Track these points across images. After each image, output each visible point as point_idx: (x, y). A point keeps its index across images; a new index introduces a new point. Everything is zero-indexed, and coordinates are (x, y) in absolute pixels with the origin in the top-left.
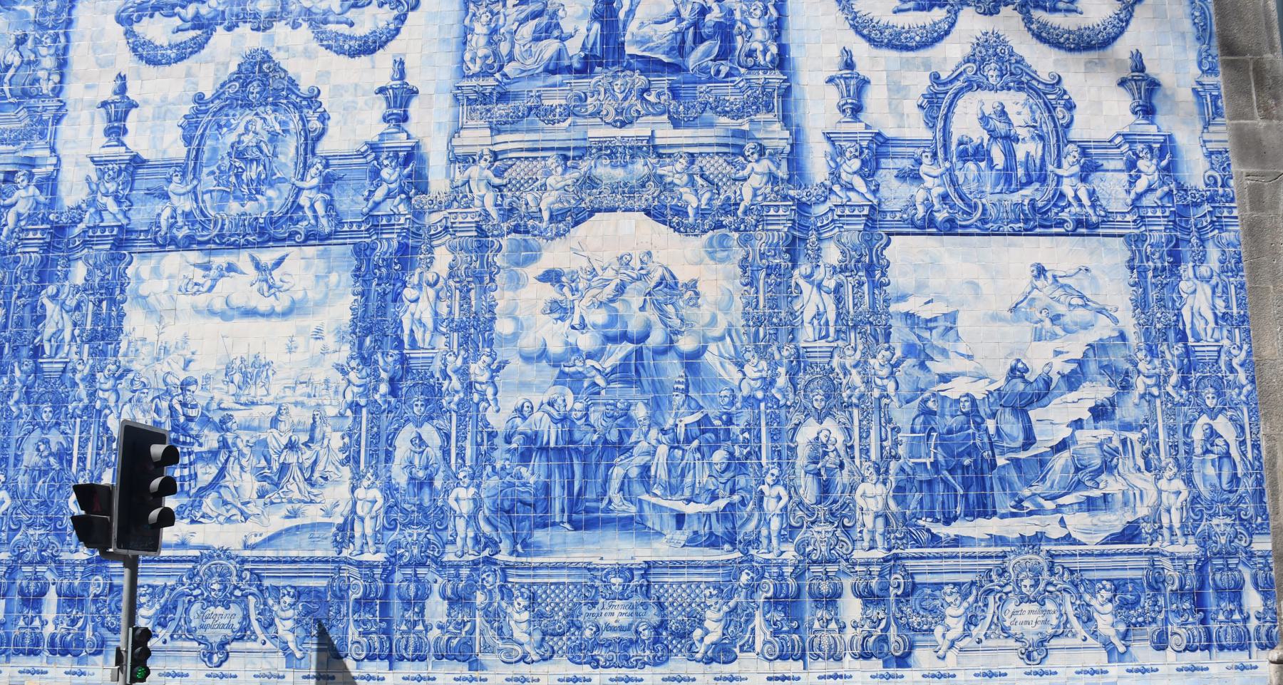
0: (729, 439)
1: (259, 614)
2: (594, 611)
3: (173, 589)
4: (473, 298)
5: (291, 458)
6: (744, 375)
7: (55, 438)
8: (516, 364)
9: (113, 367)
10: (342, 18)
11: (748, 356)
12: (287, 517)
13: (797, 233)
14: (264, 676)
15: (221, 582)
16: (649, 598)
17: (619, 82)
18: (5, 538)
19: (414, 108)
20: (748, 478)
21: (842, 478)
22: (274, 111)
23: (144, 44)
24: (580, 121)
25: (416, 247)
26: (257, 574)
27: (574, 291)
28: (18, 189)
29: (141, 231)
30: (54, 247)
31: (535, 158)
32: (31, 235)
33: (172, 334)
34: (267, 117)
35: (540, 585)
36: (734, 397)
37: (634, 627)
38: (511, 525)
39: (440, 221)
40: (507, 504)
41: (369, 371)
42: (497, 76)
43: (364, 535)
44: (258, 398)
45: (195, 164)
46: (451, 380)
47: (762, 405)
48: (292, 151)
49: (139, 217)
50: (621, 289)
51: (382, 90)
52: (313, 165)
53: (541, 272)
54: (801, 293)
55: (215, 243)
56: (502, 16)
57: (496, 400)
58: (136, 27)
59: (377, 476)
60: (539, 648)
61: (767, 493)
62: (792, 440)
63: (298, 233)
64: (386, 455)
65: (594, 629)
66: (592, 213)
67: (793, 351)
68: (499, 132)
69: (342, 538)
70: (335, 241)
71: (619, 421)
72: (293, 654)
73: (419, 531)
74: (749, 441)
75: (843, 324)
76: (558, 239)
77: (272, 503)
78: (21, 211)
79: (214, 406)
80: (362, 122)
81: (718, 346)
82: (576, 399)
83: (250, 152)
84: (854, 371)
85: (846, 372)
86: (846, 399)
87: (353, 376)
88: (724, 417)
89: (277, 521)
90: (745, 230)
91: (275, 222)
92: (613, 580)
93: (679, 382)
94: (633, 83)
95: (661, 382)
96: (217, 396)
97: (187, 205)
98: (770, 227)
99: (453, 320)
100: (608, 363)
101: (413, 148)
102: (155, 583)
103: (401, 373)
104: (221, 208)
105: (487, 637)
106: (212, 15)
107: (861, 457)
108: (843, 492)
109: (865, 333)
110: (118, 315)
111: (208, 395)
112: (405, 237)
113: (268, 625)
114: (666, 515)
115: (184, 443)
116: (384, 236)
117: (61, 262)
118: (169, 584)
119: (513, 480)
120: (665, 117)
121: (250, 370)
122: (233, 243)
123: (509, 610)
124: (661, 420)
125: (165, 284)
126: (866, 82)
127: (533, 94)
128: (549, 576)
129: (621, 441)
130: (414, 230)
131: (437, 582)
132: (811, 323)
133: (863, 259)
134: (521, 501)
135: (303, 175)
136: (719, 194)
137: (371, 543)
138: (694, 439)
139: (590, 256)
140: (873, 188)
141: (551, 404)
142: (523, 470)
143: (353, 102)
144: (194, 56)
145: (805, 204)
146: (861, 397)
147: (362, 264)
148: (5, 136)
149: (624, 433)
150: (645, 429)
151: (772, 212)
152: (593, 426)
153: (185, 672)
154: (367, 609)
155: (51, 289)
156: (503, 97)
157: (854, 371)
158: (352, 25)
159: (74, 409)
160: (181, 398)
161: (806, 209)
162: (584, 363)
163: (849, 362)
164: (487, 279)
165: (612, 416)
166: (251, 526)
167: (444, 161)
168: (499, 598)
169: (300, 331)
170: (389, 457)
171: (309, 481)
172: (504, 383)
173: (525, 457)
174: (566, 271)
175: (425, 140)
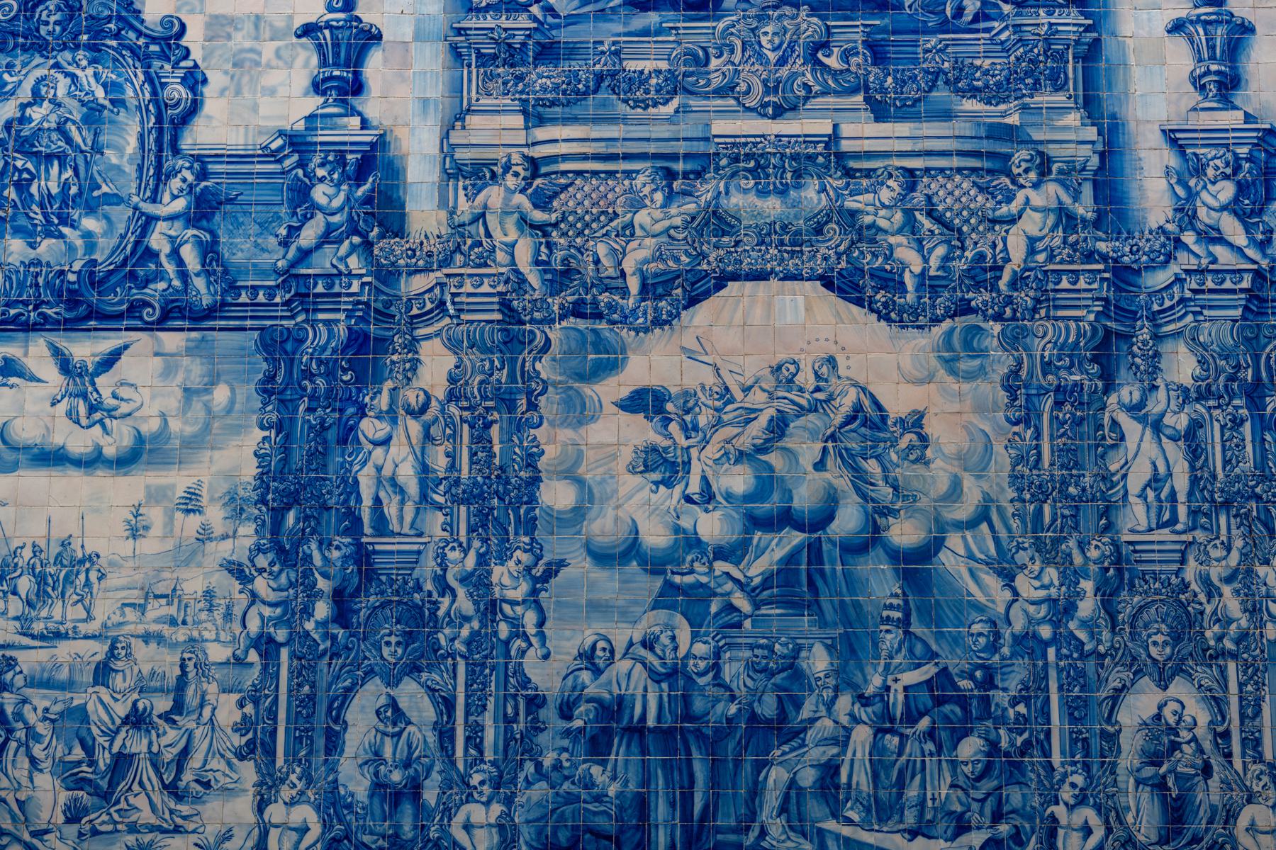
0: (989, 716)
4: (496, 440)
5: (138, 745)
6: (1016, 593)
8: (579, 567)
11: (1022, 557)
13: (1112, 325)
17: (769, 29)
19: (375, 66)
20: (1026, 791)
21: (1210, 794)
22: (93, 62)
24: (694, 102)
25: (384, 340)
31: (611, 174)
34: (79, 72)
36: (997, 635)
39: (430, 290)
41: (293, 576)
42: (535, 9)
44: (69, 625)
46: (454, 595)
47: (1051, 652)
48: (132, 144)
50: (779, 427)
51: (308, 30)
52: (174, 172)
53: (625, 392)
54: (1122, 438)
57: (542, 636)
59: (310, 781)
61: (1063, 820)
62: (1108, 720)
63: (147, 304)
64: (328, 739)
67: (1108, 550)
68: (541, 121)
71: (778, 679)
74: (1026, 720)
75: (1204, 500)
76: (657, 331)
77: (95, 833)
80: (272, 92)
81: (964, 538)
82: (695, 637)
83: (45, 142)
84: (1227, 590)
85: (1212, 591)
86: (1212, 643)
87: (261, 585)
88: (978, 674)
90: (1014, 318)
91: (101, 282)
93: (891, 607)
94: (797, 32)
95: (857, 605)
98: (1060, 313)
99: (457, 482)
100: (757, 569)
101: (373, 145)
103: (356, 580)
107: (1244, 755)
108: (1210, 822)
109: (1247, 515)
112: (361, 319)
116: (321, 316)
119: (575, 790)
120: (859, 98)
121: (51, 570)
124: (858, 679)
126: (1247, 29)
127: (605, 48)
129: (782, 716)
130: (380, 306)
132: (1142, 495)
133: (1241, 375)
134: (590, 830)
135: (155, 191)
136: (963, 249)
138: (921, 715)
139: (719, 363)
140: (1260, 237)
142: (596, 770)
143: (251, 50)
145: (1128, 268)
146: (1242, 637)
147: (277, 369)
150: (828, 694)
151: (1065, 284)
152: (728, 688)
156: (548, 52)
157: (1227, 590)
161: (1132, 278)
162: (711, 569)
163: (1215, 573)
164: (522, 403)
167: (435, 176)
169: (155, 495)
170: (334, 743)
171: (173, 790)
172: (558, 603)
173: (598, 746)
174: (674, 390)
175: (400, 132)
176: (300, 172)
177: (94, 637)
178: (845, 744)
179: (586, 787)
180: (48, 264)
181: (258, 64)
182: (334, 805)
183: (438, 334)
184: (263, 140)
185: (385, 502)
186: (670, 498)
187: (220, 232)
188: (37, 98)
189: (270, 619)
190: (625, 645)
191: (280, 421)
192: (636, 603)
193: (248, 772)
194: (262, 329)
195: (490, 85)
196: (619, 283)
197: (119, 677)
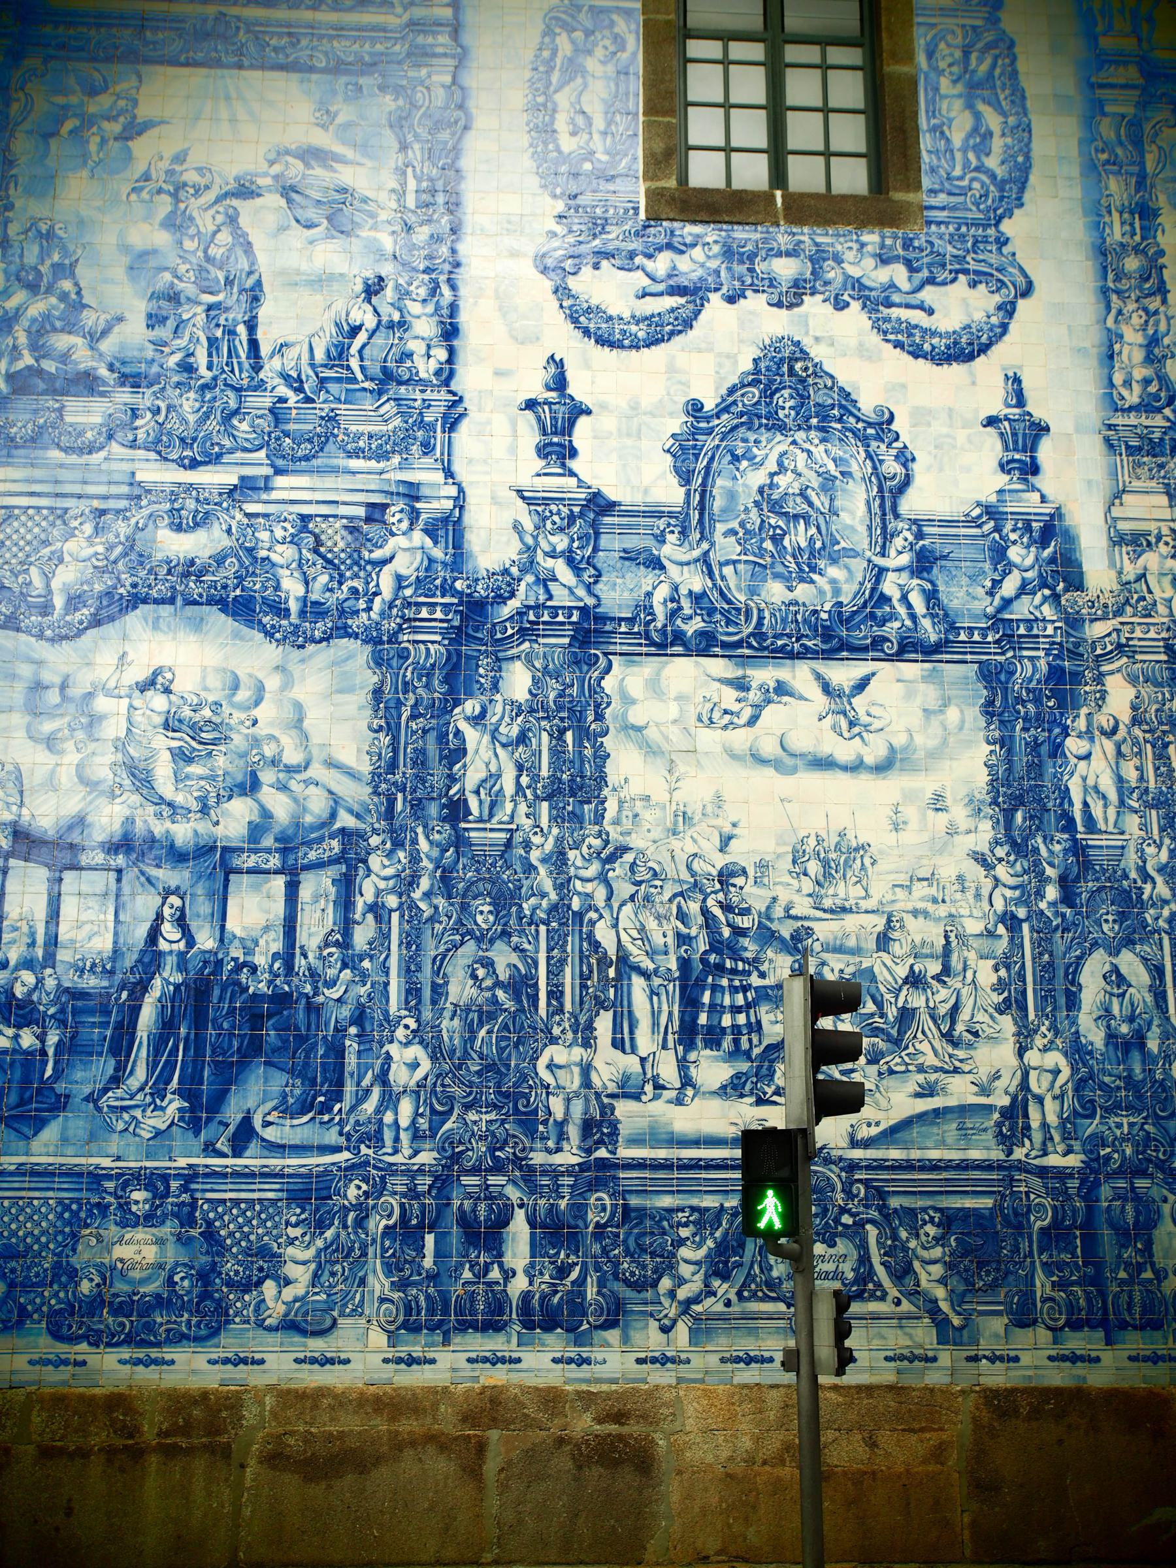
1: (885, 1254)
5: (917, 1001)
7: (504, 958)
9: (597, 843)
10: (911, 299)
12: (918, 1095)
14: (902, 1358)
18: (426, 1126)
19: (1046, 452)
22: (823, 440)
23: (589, 310)
28: (393, 534)
29: (621, 619)
30: (467, 634)
32: (424, 614)
34: (812, 448)
39: (1109, 635)
41: (1026, 866)
43: (1045, 1125)
44: (852, 902)
45: (701, 514)
46: (1154, 883)
48: (861, 509)
49: (615, 595)
51: (991, 421)
55: (750, 646)
56: (1162, 317)
58: (572, 282)
64: (1067, 997)
70: (948, 657)
72: (947, 1320)
73: (1132, 1119)
77: (891, 1072)
78: (404, 572)
79: (778, 912)
83: (791, 504)
87: (1001, 871)
91: (848, 620)
96: (784, 896)
97: (696, 582)
99: (1146, 790)
101: (1052, 516)
102: (704, 1204)
103: (1076, 869)
104: (753, 592)
106: (700, 272)
110: (595, 756)
111: (767, 894)
112: (1056, 657)
113: (902, 1272)
115: (734, 971)
116: (1025, 653)
118: (727, 1205)
121: (833, 855)
125: (673, 710)
130: (1071, 646)
135: (884, 547)
137: (1057, 1138)
143: (948, 436)
144: (677, 339)
147: (995, 695)
148: (361, 444)
153: (767, 1354)
155: (471, 706)
158: (930, 312)
159: (534, 910)
167: (1104, 542)
169: (909, 796)
170: (1073, 1002)
171: (949, 1037)
176: (997, 536)
180: (804, 605)
181: (954, 447)
182: (1078, 1051)
183: (1119, 670)
184: (966, 509)
185: (1092, 805)
187: (939, 583)
188: (782, 468)
189: (1012, 899)
191: (1002, 738)
194: (980, 663)
195: (1139, 471)
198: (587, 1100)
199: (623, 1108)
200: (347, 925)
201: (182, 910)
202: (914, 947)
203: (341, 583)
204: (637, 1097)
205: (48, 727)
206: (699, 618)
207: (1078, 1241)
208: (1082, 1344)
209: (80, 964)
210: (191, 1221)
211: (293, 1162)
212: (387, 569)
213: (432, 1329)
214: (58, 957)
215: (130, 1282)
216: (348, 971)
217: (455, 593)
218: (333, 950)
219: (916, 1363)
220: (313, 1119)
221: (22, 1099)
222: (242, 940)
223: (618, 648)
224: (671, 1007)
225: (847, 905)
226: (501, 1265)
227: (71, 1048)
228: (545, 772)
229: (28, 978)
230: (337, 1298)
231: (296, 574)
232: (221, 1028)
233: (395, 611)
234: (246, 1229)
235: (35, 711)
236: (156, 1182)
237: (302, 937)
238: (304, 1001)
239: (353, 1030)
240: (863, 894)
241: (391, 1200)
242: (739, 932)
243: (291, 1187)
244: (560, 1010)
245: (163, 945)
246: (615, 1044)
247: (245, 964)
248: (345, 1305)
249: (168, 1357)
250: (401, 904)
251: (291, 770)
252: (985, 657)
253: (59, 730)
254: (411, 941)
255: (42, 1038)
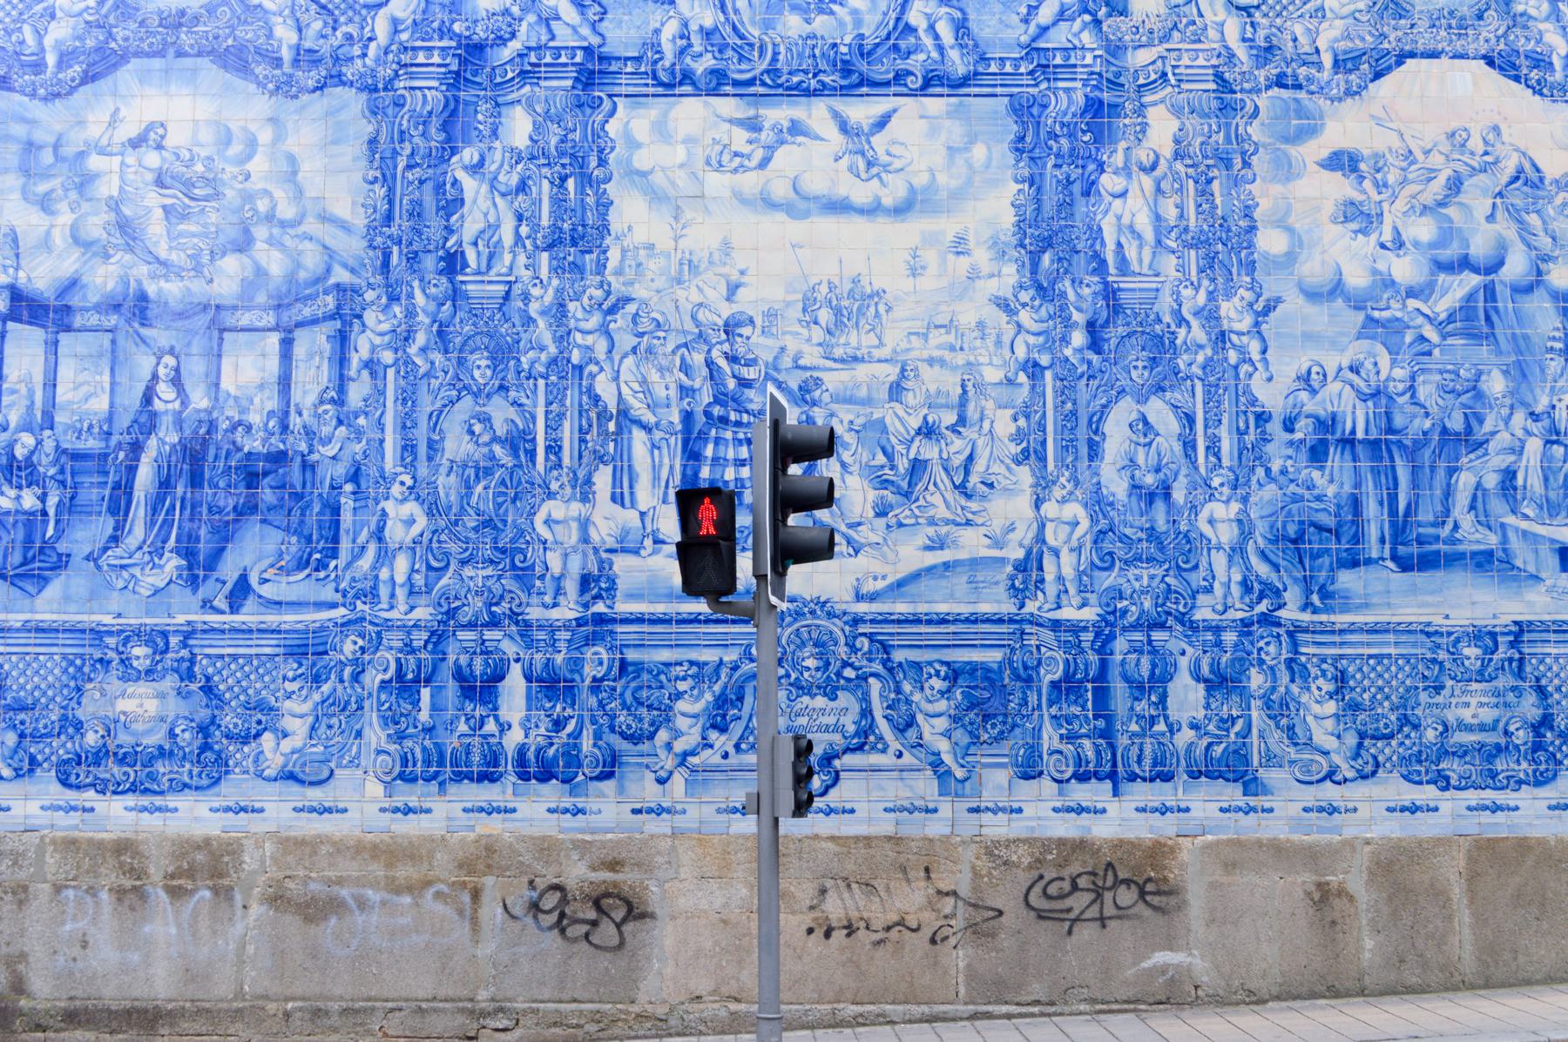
1: (889, 707)
2: (1439, 699)
3: (735, 668)
5: (930, 451)
8: (1293, 303)
9: (598, 293)
12: (928, 548)
14: (902, 809)
15: (819, 656)
16: (1523, 679)
18: (422, 582)
25: (1116, 106)
26: (881, 642)
27: (1381, 186)
29: (627, 59)
30: (466, 79)
32: (421, 59)
33: (702, 237)
35: (1352, 659)
37: (1501, 725)
38: (1301, 562)
39: (1153, 62)
40: (1292, 530)
43: (1060, 579)
44: (864, 351)
49: (618, 33)
50: (1455, 185)
53: (1325, 153)
55: (764, 84)
57: (1265, 361)
59: (1077, 484)
60: (1354, 759)
65: (1440, 728)
66: (1401, 58)
69: (1024, 582)
71: (1464, 398)
72: (949, 772)
73: (1152, 571)
76: (1349, 100)
77: (901, 525)
78: (400, 14)
79: (787, 362)
82: (1394, 363)
87: (1025, 317)
89: (910, 555)
91: (870, 53)
92: (1467, 651)
93: (1554, 339)
95: (1526, 337)
96: (792, 346)
99: (1186, 230)
103: (1105, 314)
104: (768, 25)
105: (1270, 741)
110: (598, 204)
113: (905, 725)
114: (1544, 549)
115: (738, 424)
116: (1061, 84)
117: (483, 107)
118: (726, 659)
119: (1299, 491)
121: (845, 303)
122: (797, 86)
123: (1304, 698)
124: (1529, 399)
125: (681, 153)
128: (1369, 645)
129: (1469, 430)
130: (1110, 76)
131: (1185, 654)
137: (1072, 590)
141: (1355, 369)
142: (1316, 474)
147: (1026, 130)
149: (1473, 418)
150: (1505, 412)
154: (1073, 698)
155: (469, 154)
160: (726, 347)
162: (1404, 306)
165: (1452, 391)
166: (863, 562)
168: (1284, 677)
169: (930, 240)
170: (1094, 451)
171: (962, 489)
173: (1317, 454)
174: (1366, 152)
177: (886, 361)
178: (1521, 453)
179: (1308, 488)
180: (823, 38)
182: (1098, 502)
185: (1126, 246)
186: (1367, 244)
187: (969, 10)
189: (1035, 346)
190: (1335, 369)
192: (1344, 334)
193: (1025, 475)
196: (1315, 58)
197: (910, 394)
198: (585, 555)
199: (621, 563)
200: (342, 383)
201: (177, 370)
202: (929, 397)
203: (334, 29)
204: (636, 552)
205: (42, 188)
206: (709, 55)
207: (1090, 695)
208: (1088, 795)
209: (78, 425)
210: (191, 676)
211: (289, 619)
212: (382, 12)
213: (427, 780)
214: (57, 419)
215: (134, 734)
216: (343, 428)
217: (453, 35)
218: (328, 407)
219: (916, 814)
220: (309, 575)
221: (25, 557)
222: (236, 399)
223: (623, 90)
224: (672, 463)
225: (859, 354)
226: (496, 718)
227: (70, 506)
228: (545, 222)
229: (28, 440)
230: (334, 750)
231: (289, 21)
232: (216, 486)
233: (391, 56)
234: (244, 684)
235: (26, 172)
236: (157, 639)
237: (296, 395)
238: (299, 459)
239: (349, 487)
240: (876, 342)
241: (388, 655)
242: (744, 383)
243: (288, 642)
244: (559, 465)
245: (158, 405)
246: (613, 499)
247: (240, 423)
248: (342, 757)
249: (171, 805)
250: (397, 360)
251: (283, 224)
252: (1016, 90)
253: (53, 191)
254: (407, 398)
255: (43, 498)
